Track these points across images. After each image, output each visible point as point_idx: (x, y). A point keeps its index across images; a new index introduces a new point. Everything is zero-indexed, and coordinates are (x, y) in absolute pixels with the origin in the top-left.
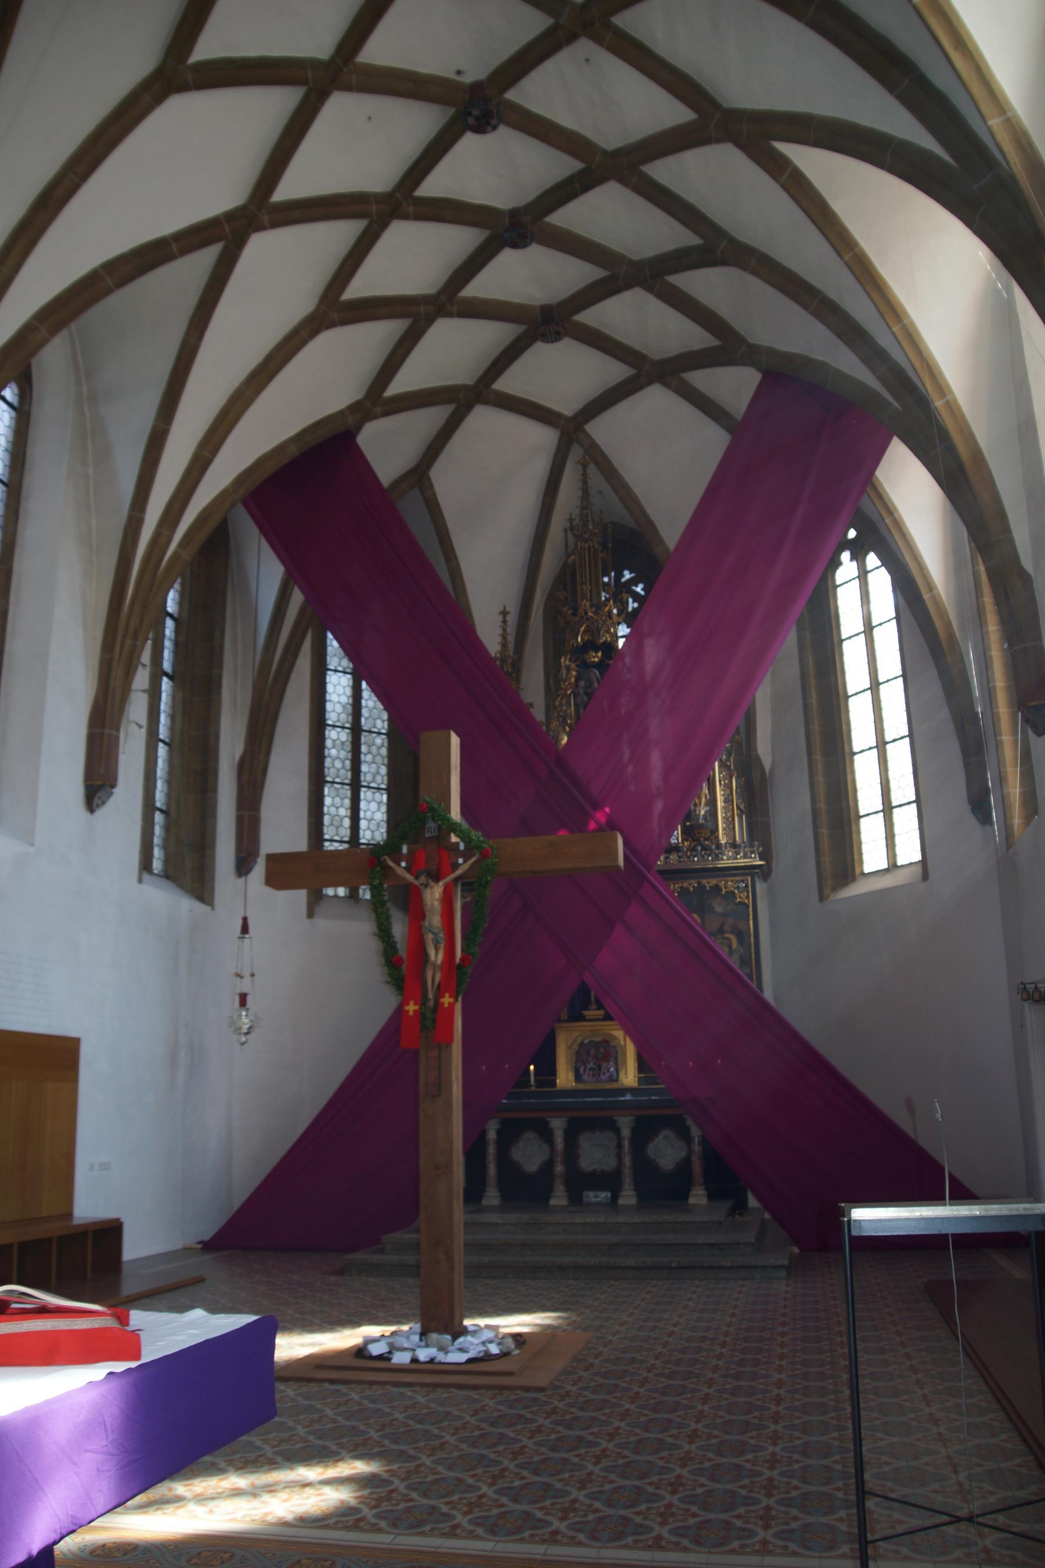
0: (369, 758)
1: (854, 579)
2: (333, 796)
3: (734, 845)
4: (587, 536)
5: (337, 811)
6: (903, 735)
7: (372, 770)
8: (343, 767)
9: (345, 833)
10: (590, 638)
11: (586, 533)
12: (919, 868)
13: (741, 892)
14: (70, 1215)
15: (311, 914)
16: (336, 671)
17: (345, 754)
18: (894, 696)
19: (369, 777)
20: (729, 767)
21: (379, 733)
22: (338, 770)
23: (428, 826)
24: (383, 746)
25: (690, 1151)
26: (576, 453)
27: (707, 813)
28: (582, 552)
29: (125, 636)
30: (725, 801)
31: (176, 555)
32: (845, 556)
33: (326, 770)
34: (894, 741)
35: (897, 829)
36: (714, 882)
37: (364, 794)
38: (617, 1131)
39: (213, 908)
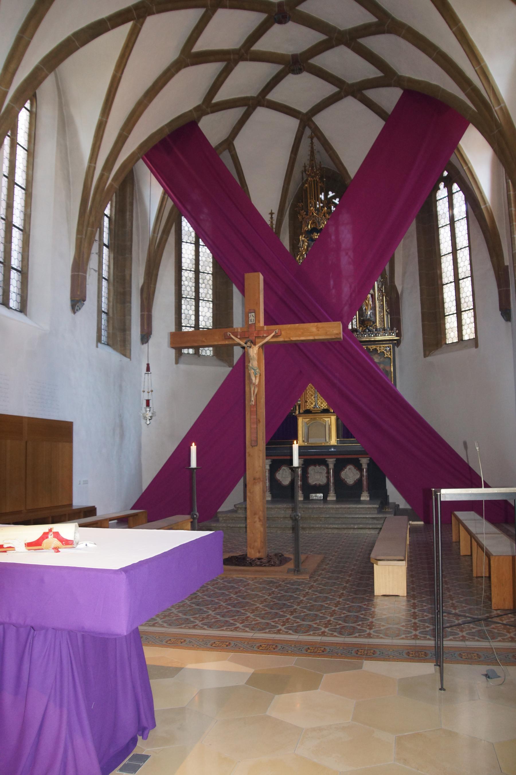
0: (203, 286)
1: (445, 197)
2: (186, 304)
3: (384, 329)
4: (313, 174)
5: (188, 312)
6: (467, 276)
7: (205, 292)
8: (191, 290)
9: (192, 323)
10: (315, 226)
11: (312, 173)
13: (388, 352)
14: (71, 505)
15: (177, 362)
16: (187, 242)
17: (192, 284)
18: (464, 256)
19: (203, 295)
20: (382, 291)
21: (208, 273)
22: (188, 292)
23: (250, 318)
24: (210, 280)
25: (362, 476)
26: (308, 132)
27: (371, 313)
28: (311, 183)
29: (87, 227)
30: (379, 308)
31: (111, 185)
32: (442, 185)
33: (183, 292)
34: (463, 279)
35: (464, 322)
36: (374, 347)
37: (201, 303)
38: (327, 466)
39: (131, 360)
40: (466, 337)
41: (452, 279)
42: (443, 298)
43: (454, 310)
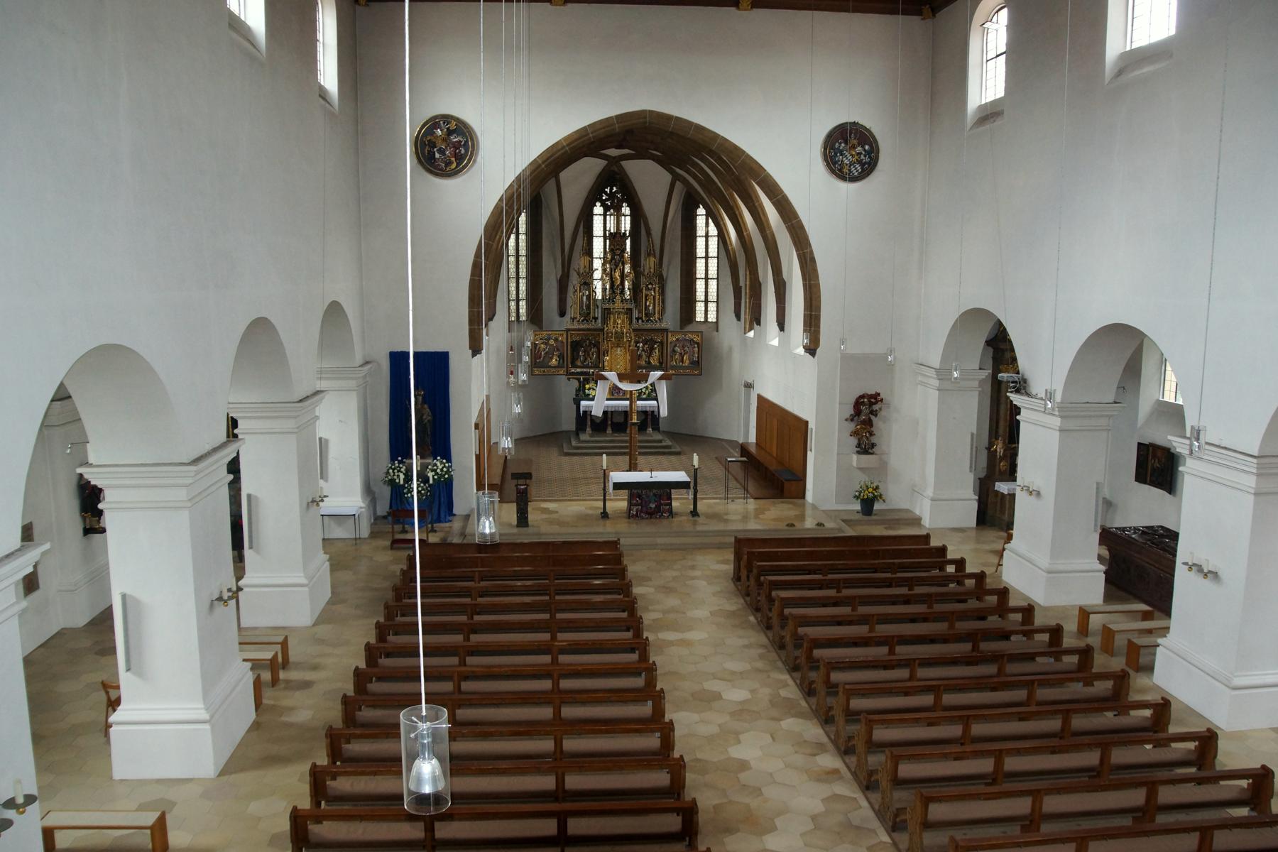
12: (715, 325)
15: (509, 332)
18: (713, 264)
32: (701, 206)
35: (709, 309)
37: (520, 280)
40: (710, 320)
41: (703, 276)
42: (696, 288)
43: (703, 298)
